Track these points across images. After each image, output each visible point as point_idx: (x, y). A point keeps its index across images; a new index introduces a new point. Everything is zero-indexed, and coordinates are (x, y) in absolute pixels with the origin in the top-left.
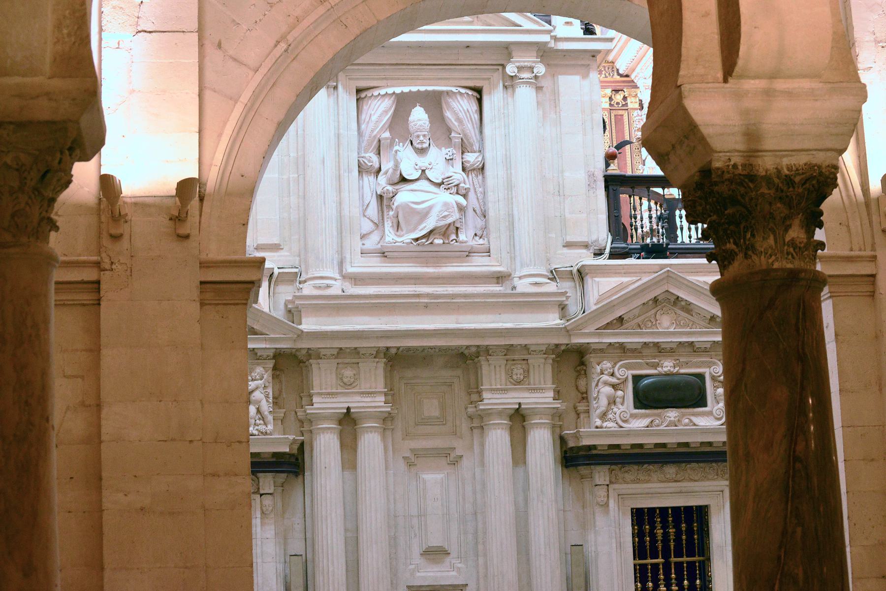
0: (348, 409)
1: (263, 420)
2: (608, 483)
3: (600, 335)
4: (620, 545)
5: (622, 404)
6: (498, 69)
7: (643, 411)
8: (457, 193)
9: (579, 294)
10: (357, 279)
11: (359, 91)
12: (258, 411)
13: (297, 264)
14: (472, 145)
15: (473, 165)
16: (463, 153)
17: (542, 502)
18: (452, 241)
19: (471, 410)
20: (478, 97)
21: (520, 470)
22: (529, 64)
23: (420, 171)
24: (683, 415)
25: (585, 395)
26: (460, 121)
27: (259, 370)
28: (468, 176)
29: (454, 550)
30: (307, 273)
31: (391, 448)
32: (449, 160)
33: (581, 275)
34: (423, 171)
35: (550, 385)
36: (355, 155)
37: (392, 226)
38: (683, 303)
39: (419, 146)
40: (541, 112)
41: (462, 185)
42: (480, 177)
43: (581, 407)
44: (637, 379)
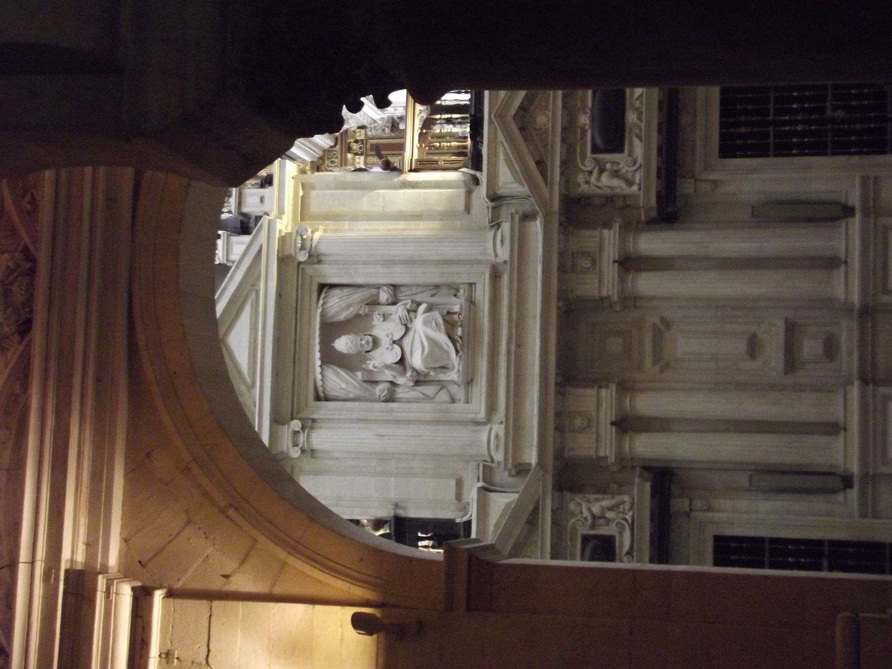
0: (612, 423)
1: (620, 504)
2: (693, 181)
3: (552, 184)
4: (755, 170)
5: (618, 164)
6: (302, 268)
8: (415, 311)
9: (514, 201)
10: (491, 408)
11: (318, 398)
12: (611, 509)
13: (475, 464)
14: (373, 295)
15: (391, 296)
16: (379, 304)
18: (459, 318)
19: (618, 307)
20: (327, 288)
24: (632, 105)
25: (609, 200)
26: (348, 307)
27: (572, 507)
28: (400, 300)
30: (482, 455)
32: (385, 317)
33: (496, 198)
34: (394, 342)
35: (596, 233)
36: (377, 405)
37: (444, 373)
38: (526, 103)
39: (371, 345)
41: (408, 306)
42: (402, 289)
43: (620, 203)
44: (595, 150)
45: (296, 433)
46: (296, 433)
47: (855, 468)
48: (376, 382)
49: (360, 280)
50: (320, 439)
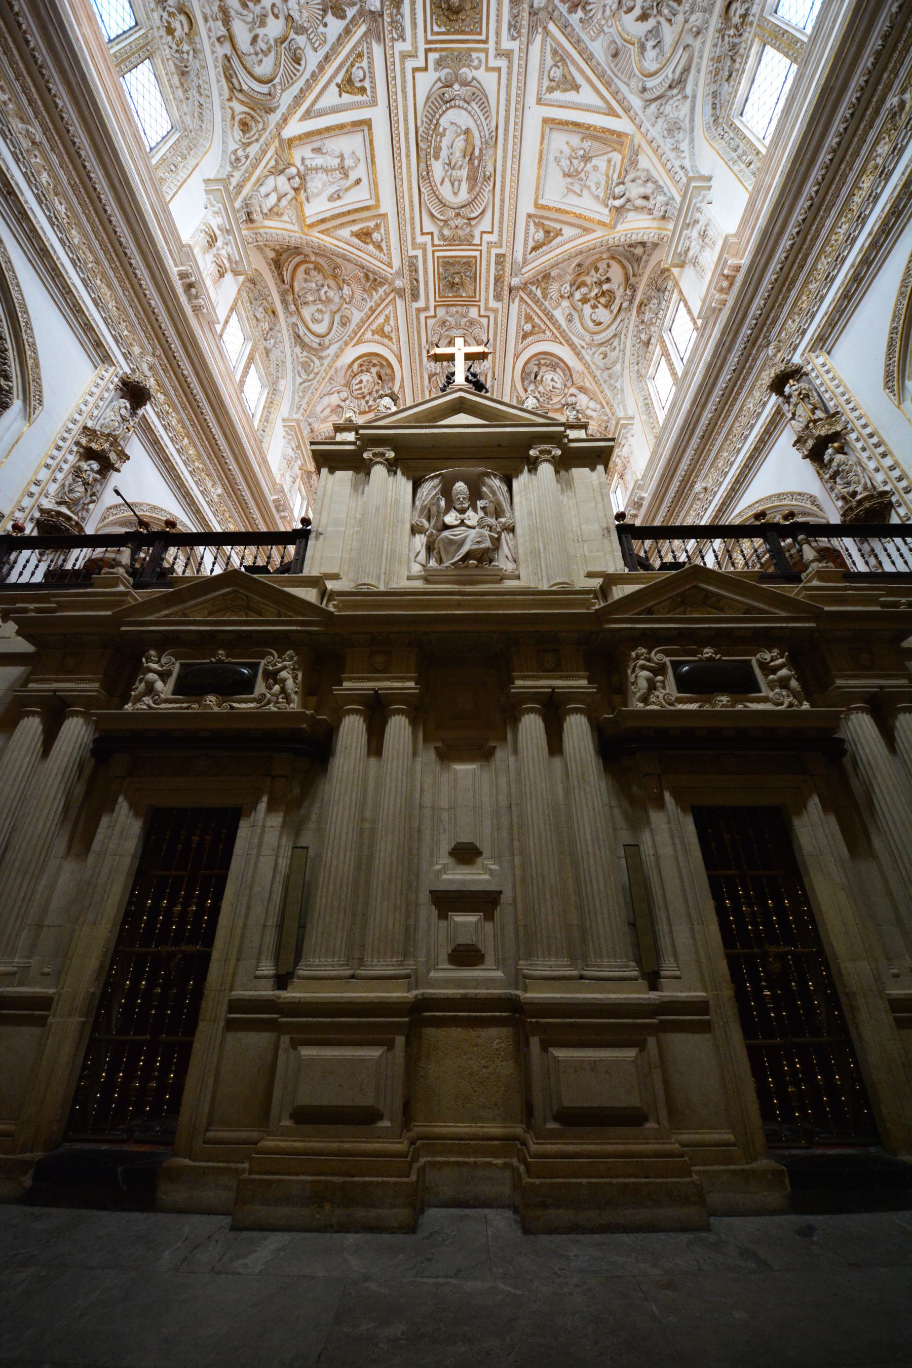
5: (664, 688)
7: (689, 695)
8: (490, 531)
17: (585, 790)
21: (557, 761)
26: (494, 493)
29: (486, 848)
31: (421, 735)
33: (604, 591)
34: (462, 521)
40: (559, 487)
42: (511, 535)
46: (383, 455)
47: (293, 994)
48: (429, 521)
49: (516, 499)
50: (379, 472)
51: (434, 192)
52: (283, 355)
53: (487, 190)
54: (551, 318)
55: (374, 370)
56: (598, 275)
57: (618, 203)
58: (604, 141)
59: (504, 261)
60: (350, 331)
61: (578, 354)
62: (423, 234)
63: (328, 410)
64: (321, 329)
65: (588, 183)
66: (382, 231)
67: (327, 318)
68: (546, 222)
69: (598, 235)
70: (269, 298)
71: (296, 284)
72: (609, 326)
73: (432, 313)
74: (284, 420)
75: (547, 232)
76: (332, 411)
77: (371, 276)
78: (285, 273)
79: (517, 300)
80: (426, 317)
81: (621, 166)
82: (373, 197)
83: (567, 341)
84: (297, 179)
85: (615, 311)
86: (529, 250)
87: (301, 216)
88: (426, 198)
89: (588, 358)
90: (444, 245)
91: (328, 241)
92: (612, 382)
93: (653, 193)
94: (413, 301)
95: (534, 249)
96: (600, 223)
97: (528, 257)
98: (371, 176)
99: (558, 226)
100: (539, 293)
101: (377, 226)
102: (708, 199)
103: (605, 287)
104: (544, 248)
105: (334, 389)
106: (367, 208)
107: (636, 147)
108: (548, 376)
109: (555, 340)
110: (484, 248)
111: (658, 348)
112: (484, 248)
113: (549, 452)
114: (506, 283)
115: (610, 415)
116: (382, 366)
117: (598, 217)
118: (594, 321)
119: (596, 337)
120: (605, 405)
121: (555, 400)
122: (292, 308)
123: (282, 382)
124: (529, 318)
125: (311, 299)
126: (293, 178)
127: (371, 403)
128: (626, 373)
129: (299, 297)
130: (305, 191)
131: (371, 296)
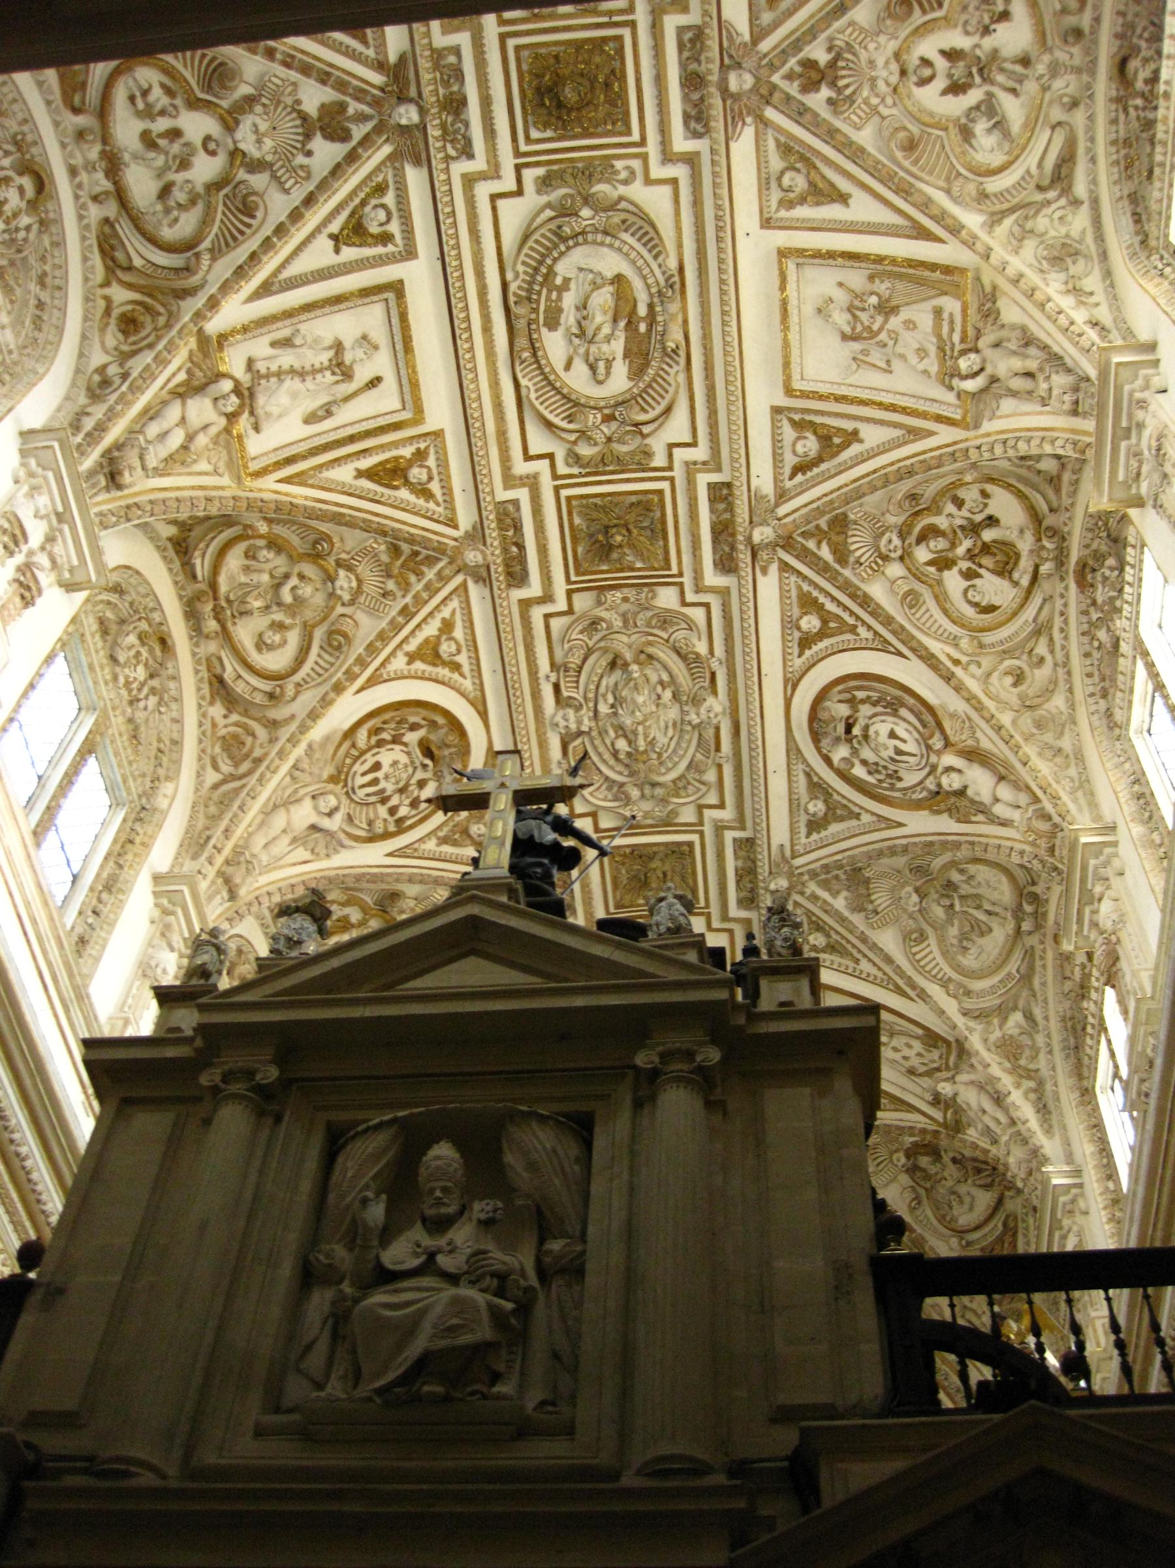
8: (500, 1293)
16: (542, 1241)
18: (472, 1394)
22: (684, 1047)
23: (423, 1258)
26: (532, 1166)
34: (432, 1256)
45: (250, 1074)
46: (250, 1074)
51: (550, 383)
52: (175, 727)
53: (672, 372)
54: (865, 601)
55: (412, 738)
56: (964, 513)
57: (970, 385)
58: (920, 282)
59: (731, 494)
60: (351, 661)
61: (948, 678)
62: (528, 457)
63: (286, 840)
64: (276, 661)
65: (899, 349)
66: (431, 462)
67: (293, 638)
68: (818, 420)
69: (945, 435)
70: (156, 617)
71: (222, 580)
72: (1015, 614)
73: (562, 605)
74: (157, 878)
75: (825, 439)
76: (294, 840)
77: (405, 548)
78: (198, 562)
79: (774, 568)
80: (547, 616)
81: (964, 321)
82: (409, 404)
83: (913, 650)
84: (234, 399)
85: (1025, 582)
86: (787, 471)
87: (237, 464)
88: (533, 396)
89: (974, 686)
90: (581, 475)
91: (299, 493)
92: (1049, 737)
93: (1041, 369)
94: (509, 586)
95: (798, 469)
96: (939, 419)
97: (788, 484)
98: (403, 372)
99: (848, 425)
100: (825, 553)
101: (420, 455)
102: (1156, 382)
103: (988, 535)
104: (824, 466)
105: (302, 792)
106: (396, 426)
107: (988, 289)
108: (881, 728)
109: (884, 647)
110: (678, 473)
111: (1140, 665)
112: (678, 473)
113: (690, 1055)
114: (740, 538)
115: (1057, 819)
116: (433, 724)
117: (934, 409)
118: (975, 605)
119: (989, 638)
120: (1039, 793)
121: (910, 779)
122: (212, 625)
123: (167, 788)
124: (809, 604)
125: (258, 604)
126: (224, 397)
127: (403, 811)
128: (1082, 714)
129: (228, 601)
130: (252, 413)
131: (406, 587)
